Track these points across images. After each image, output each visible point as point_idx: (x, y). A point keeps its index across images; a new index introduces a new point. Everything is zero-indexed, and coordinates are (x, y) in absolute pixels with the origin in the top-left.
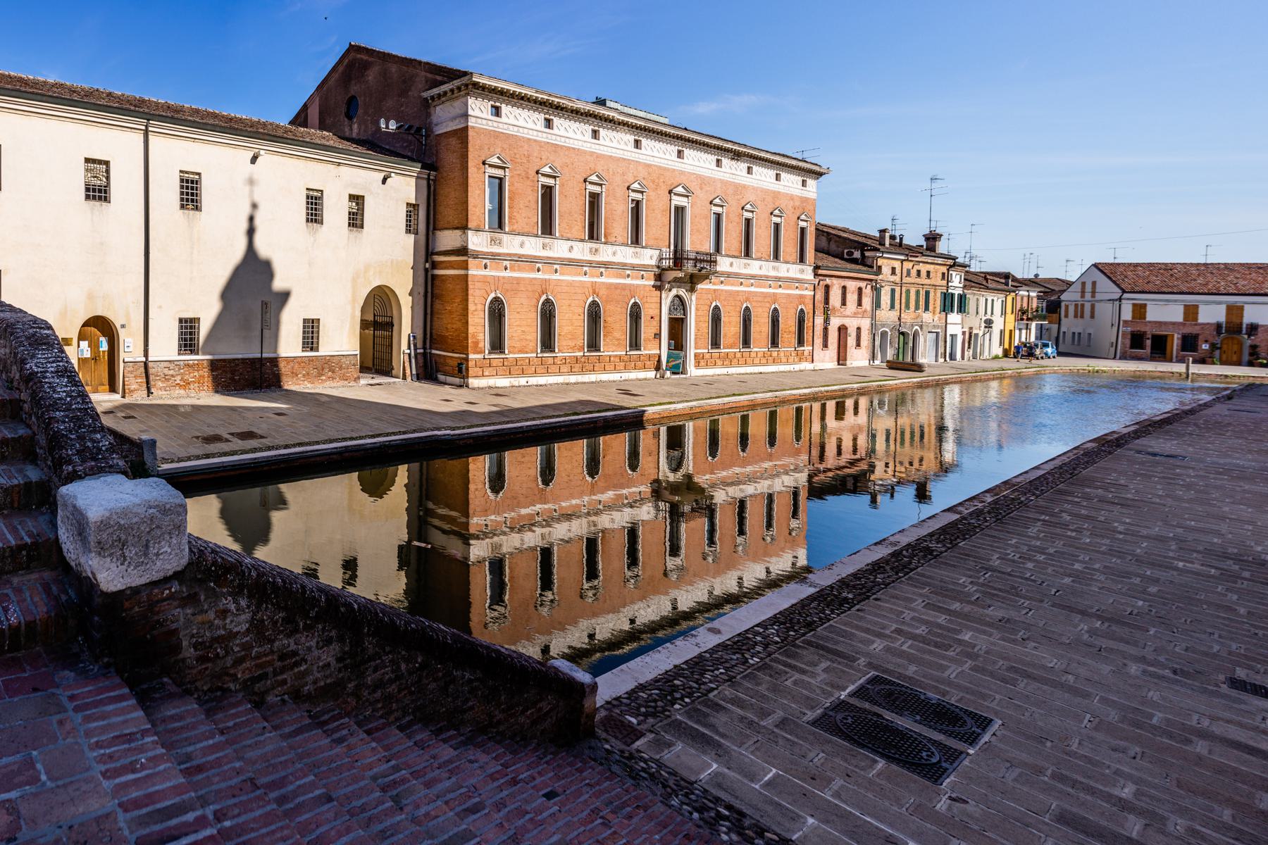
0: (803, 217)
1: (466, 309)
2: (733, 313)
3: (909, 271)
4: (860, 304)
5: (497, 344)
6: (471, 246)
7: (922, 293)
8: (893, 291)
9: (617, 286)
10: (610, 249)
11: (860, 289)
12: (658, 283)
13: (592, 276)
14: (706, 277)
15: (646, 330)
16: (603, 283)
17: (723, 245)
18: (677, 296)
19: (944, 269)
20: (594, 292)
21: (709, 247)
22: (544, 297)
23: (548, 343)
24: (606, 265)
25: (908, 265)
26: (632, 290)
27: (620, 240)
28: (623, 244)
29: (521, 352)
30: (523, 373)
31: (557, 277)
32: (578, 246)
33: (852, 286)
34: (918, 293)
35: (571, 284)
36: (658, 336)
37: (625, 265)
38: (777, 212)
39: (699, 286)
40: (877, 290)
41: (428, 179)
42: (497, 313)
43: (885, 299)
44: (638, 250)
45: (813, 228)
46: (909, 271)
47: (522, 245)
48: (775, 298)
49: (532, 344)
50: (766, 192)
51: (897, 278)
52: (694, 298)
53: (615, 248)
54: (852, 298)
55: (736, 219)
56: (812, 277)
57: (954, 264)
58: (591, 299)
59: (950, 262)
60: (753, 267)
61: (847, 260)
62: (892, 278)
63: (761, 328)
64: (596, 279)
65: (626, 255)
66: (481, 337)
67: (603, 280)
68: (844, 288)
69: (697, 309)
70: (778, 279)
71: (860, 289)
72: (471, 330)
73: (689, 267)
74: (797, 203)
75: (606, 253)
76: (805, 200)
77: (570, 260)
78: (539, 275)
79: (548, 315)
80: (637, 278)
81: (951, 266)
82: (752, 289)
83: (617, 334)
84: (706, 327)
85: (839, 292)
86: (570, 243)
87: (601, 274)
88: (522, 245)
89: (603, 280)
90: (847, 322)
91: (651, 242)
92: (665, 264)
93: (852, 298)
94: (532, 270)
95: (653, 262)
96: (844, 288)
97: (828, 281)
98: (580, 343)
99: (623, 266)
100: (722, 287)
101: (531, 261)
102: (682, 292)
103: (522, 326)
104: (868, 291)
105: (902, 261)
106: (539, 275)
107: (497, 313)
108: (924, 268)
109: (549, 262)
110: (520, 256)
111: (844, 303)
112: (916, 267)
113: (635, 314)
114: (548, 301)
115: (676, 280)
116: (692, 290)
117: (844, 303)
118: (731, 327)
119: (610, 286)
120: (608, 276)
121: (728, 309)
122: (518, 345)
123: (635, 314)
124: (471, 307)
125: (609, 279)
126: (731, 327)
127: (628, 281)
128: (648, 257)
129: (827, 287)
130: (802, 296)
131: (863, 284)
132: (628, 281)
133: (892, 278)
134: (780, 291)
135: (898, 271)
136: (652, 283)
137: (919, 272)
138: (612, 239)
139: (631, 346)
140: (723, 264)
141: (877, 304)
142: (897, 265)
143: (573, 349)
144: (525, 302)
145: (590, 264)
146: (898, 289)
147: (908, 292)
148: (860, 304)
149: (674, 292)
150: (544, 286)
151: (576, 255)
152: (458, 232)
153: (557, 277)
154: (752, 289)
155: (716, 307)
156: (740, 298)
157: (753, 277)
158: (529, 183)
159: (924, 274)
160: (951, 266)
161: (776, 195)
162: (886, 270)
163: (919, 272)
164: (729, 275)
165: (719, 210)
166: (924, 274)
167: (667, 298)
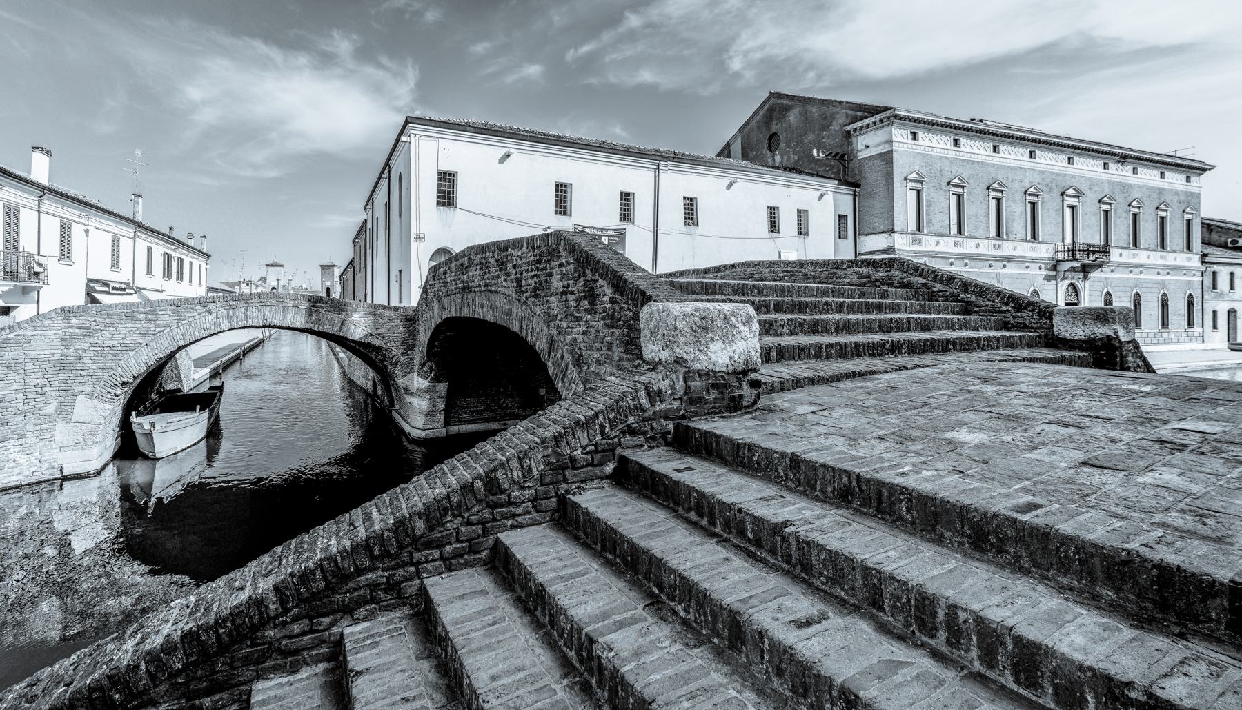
0: (1188, 210)
6: (897, 247)
10: (1010, 245)
12: (1054, 273)
17: (1113, 238)
18: (1072, 284)
21: (1098, 240)
24: (1009, 259)
27: (1020, 236)
28: (1022, 241)
32: (983, 243)
37: (1024, 258)
38: (1162, 207)
39: (1092, 275)
41: (854, 195)
45: (1199, 221)
47: (937, 243)
50: (1152, 189)
55: (1124, 215)
56: (1195, 262)
60: (1142, 257)
61: (1231, 249)
65: (1026, 250)
67: (1005, 271)
70: (1165, 267)
74: (1182, 198)
75: (1008, 249)
76: (1191, 194)
82: (1141, 276)
86: (977, 241)
92: (1060, 256)
95: (1050, 255)
99: (1022, 260)
100: (1113, 275)
110: (937, 253)
115: (1073, 269)
116: (1085, 278)
128: (1043, 251)
134: (1168, 277)
140: (1115, 255)
145: (996, 259)
149: (1067, 282)
151: (983, 250)
152: (885, 235)
155: (1108, 293)
157: (1142, 266)
161: (1161, 191)
164: (1119, 265)
165: (1108, 207)
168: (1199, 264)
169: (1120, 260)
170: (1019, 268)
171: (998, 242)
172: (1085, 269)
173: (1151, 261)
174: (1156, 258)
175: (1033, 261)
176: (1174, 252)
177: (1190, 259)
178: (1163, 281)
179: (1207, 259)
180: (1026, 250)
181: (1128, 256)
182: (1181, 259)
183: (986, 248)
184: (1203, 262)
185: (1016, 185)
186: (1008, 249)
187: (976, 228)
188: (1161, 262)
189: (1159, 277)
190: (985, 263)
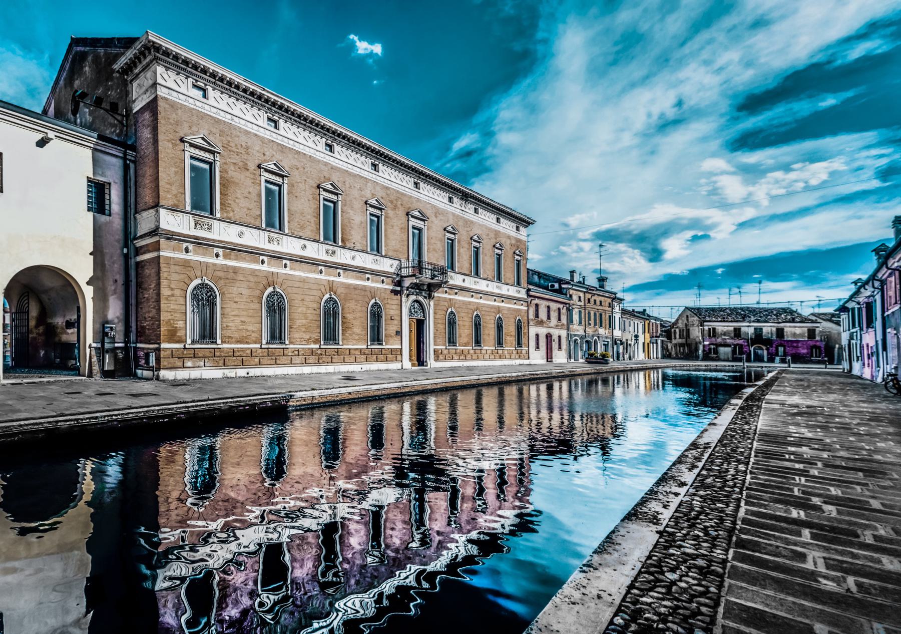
1: (159, 294)
2: (466, 319)
3: (589, 300)
4: (559, 319)
5: (207, 332)
7: (598, 315)
8: (580, 312)
9: (356, 288)
11: (559, 309)
12: (399, 289)
13: (330, 275)
14: (439, 286)
15: (388, 328)
16: (342, 283)
19: (609, 300)
20: (331, 289)
22: (270, 289)
24: (346, 268)
25: (588, 296)
26: (373, 293)
28: (362, 251)
29: (238, 342)
30: (243, 364)
31: (287, 271)
33: (554, 306)
34: (595, 314)
35: (304, 281)
36: (399, 333)
37: (364, 268)
39: (436, 294)
40: (570, 311)
42: (205, 300)
43: (576, 317)
44: (378, 258)
46: (589, 300)
48: (499, 310)
49: (254, 336)
51: (582, 304)
52: (432, 303)
53: (353, 253)
54: (554, 315)
56: (523, 295)
57: (615, 298)
58: (327, 296)
59: (613, 296)
62: (579, 303)
63: (489, 332)
64: (332, 278)
66: (180, 324)
67: (341, 279)
68: (549, 307)
69: (435, 313)
70: (500, 296)
71: (559, 309)
72: (164, 316)
73: (426, 277)
75: (343, 257)
77: (301, 257)
78: (265, 267)
79: (276, 307)
80: (377, 282)
81: (614, 299)
82: (481, 301)
83: (357, 330)
84: (444, 328)
85: (546, 310)
86: (303, 242)
87: (339, 275)
88: (241, 234)
89: (341, 279)
90: (552, 331)
91: (390, 254)
92: (404, 272)
93: (554, 315)
94: (256, 261)
95: (392, 270)
96: (549, 307)
97: (536, 301)
98: (315, 336)
99: (362, 271)
100: (456, 297)
101: (253, 253)
102: (420, 298)
103: (240, 317)
104: (564, 311)
105: (585, 293)
106: (265, 267)
107: (205, 300)
108: (598, 299)
109: (277, 257)
111: (549, 318)
112: (593, 298)
113: (376, 315)
114: (275, 293)
116: (430, 297)
117: (549, 318)
118: (464, 331)
119: (348, 287)
120: (347, 277)
121: (462, 314)
122: (236, 335)
123: (376, 315)
124: (165, 292)
125: (346, 279)
126: (464, 331)
127: (368, 283)
129: (537, 305)
130: (519, 310)
131: (561, 306)
132: (368, 283)
133: (579, 303)
135: (582, 299)
136: (391, 287)
137: (595, 301)
138: (348, 245)
139: (372, 340)
141: (570, 321)
142: (582, 295)
143: (308, 341)
144: (245, 292)
146: (583, 311)
147: (589, 313)
148: (559, 319)
149: (413, 297)
150: (271, 279)
153: (287, 271)
154: (481, 301)
156: (471, 307)
158: (248, 174)
159: (598, 303)
160: (614, 299)
162: (575, 298)
163: (595, 301)
166: (598, 303)
167: (407, 303)
168: (525, 297)
169: (463, 284)
170: (357, 278)
171: (331, 248)
172: (431, 289)
173: (489, 289)
174: (492, 287)
175: (374, 273)
176: (507, 284)
177: (519, 292)
178: (499, 307)
179: (531, 293)
180: (366, 261)
181: (470, 282)
182: (512, 291)
183: (316, 251)
184: (529, 296)
185: (355, 193)
186: (343, 257)
187: (302, 228)
188: (497, 291)
189: (496, 304)
190: (314, 267)
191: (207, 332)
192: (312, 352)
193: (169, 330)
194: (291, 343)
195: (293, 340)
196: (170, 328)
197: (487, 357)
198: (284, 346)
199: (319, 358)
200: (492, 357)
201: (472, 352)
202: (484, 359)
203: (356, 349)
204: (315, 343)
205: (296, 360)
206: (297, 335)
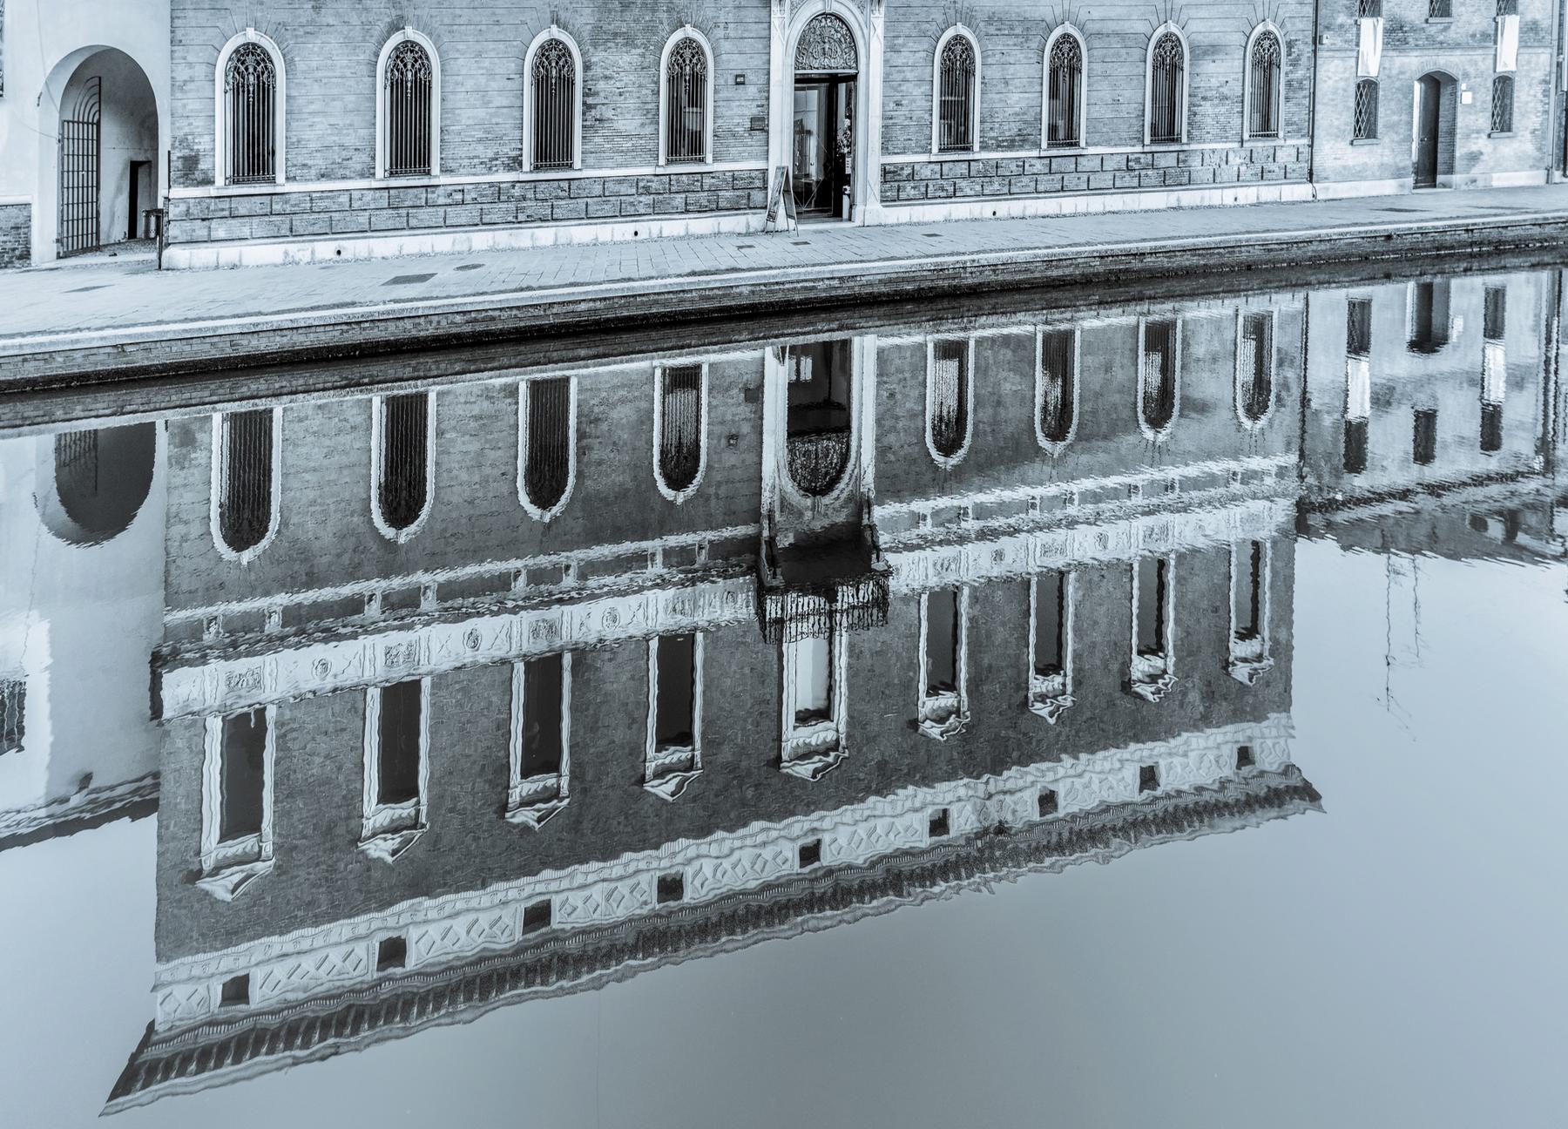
5: (254, 157)
23: (411, 151)
98: (508, 150)
191: (254, 157)
192: (498, 192)
193: (185, 158)
194: (445, 170)
195: (452, 164)
196: (186, 152)
197: (1105, 180)
198: (425, 181)
199: (520, 209)
200: (1131, 180)
201: (1039, 166)
202: (1091, 190)
203: (621, 180)
204: (510, 168)
205: (455, 215)
206: (462, 152)
